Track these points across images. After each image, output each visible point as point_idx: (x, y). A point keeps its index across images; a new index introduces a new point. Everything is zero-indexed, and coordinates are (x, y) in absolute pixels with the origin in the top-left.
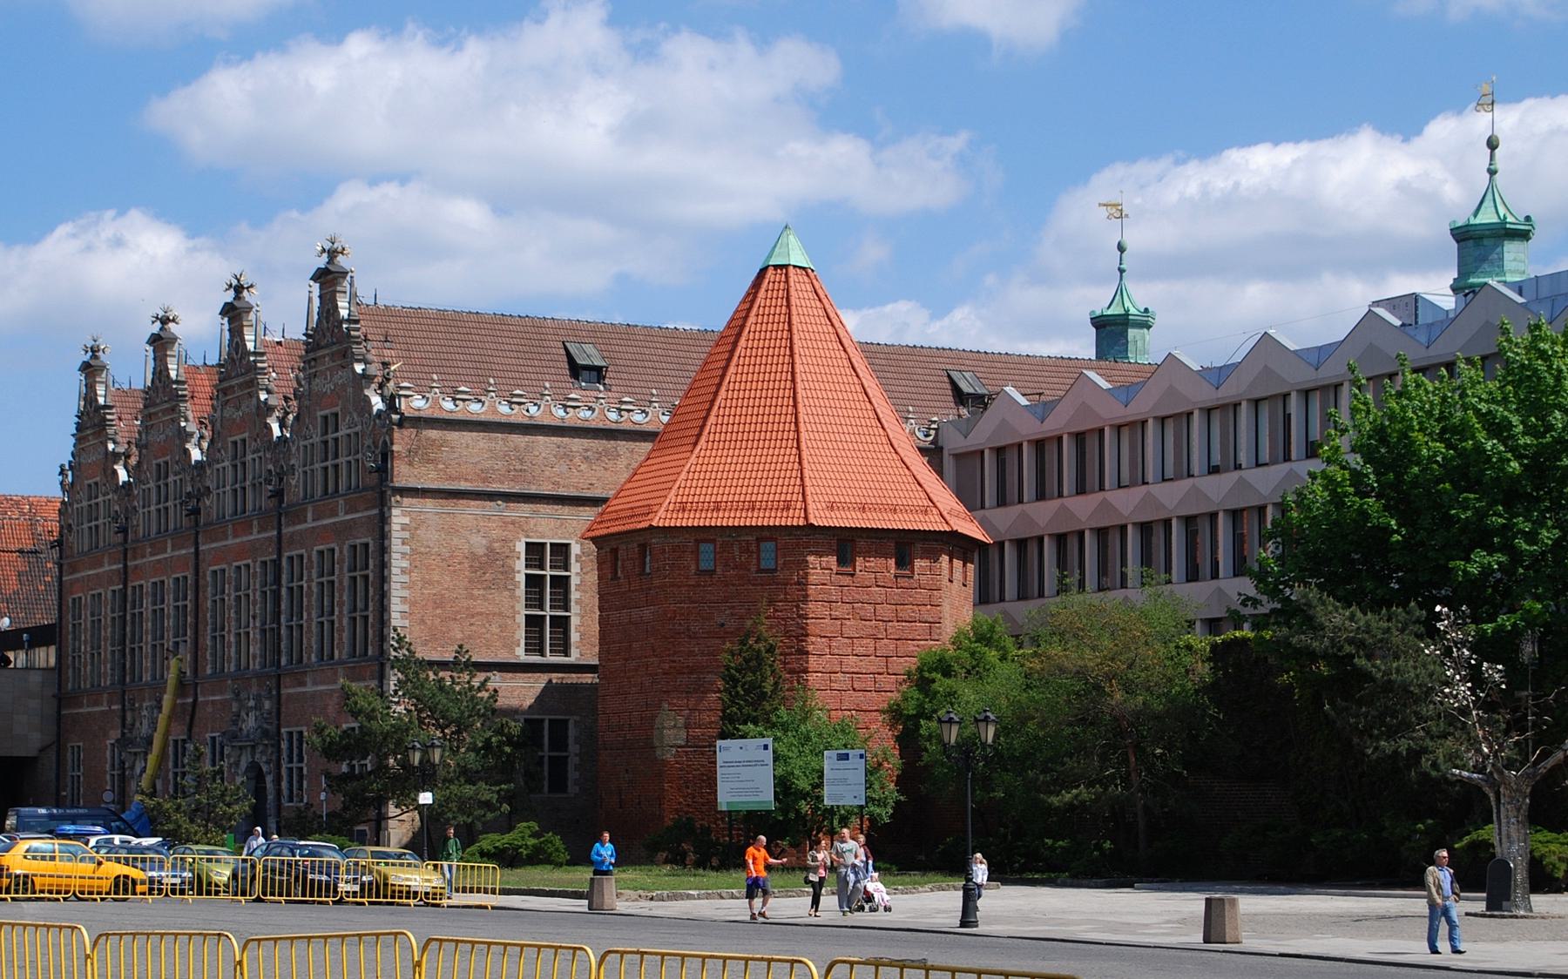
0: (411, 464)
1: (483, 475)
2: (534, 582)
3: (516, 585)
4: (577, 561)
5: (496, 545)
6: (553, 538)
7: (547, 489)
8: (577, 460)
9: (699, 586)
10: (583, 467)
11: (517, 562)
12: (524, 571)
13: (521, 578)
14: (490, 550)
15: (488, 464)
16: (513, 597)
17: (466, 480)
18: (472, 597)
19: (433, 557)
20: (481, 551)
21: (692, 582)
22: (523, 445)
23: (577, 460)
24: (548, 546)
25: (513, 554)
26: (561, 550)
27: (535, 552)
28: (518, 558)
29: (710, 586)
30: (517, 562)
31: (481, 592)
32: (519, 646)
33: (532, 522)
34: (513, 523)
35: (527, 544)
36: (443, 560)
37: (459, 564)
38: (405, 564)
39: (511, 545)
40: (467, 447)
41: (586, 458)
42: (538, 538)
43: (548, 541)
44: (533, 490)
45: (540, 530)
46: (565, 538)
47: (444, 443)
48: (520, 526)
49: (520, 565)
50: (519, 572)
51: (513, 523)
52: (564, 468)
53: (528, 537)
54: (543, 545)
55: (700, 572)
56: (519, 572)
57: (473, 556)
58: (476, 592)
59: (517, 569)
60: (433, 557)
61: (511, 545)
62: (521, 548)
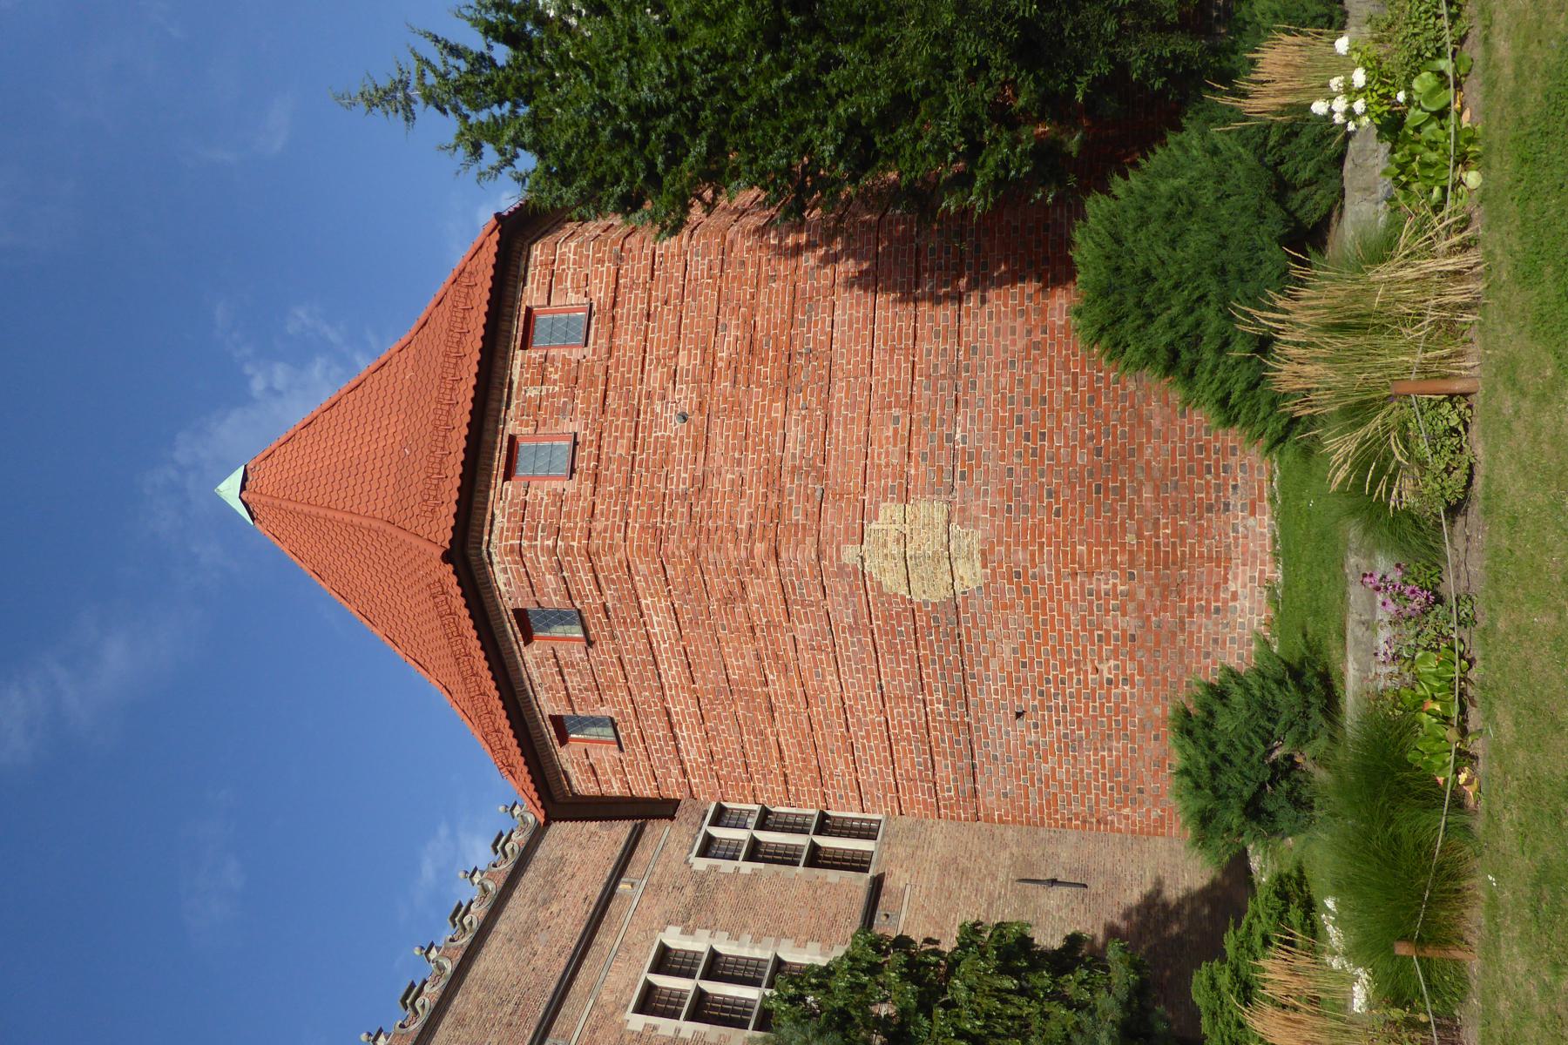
2: (703, 1009)
4: (692, 933)
8: (541, 916)
10: (555, 908)
11: (660, 1032)
23: (541, 916)
24: (661, 981)
26: (665, 961)
27: (649, 1002)
28: (655, 1028)
30: (660, 1032)
41: (545, 902)
42: (632, 991)
45: (621, 987)
48: (605, 1018)
49: (666, 1026)
50: (678, 1030)
53: (626, 1006)
54: (649, 988)
56: (678, 1030)
59: (671, 1033)
61: (627, 1038)
62: (638, 1022)
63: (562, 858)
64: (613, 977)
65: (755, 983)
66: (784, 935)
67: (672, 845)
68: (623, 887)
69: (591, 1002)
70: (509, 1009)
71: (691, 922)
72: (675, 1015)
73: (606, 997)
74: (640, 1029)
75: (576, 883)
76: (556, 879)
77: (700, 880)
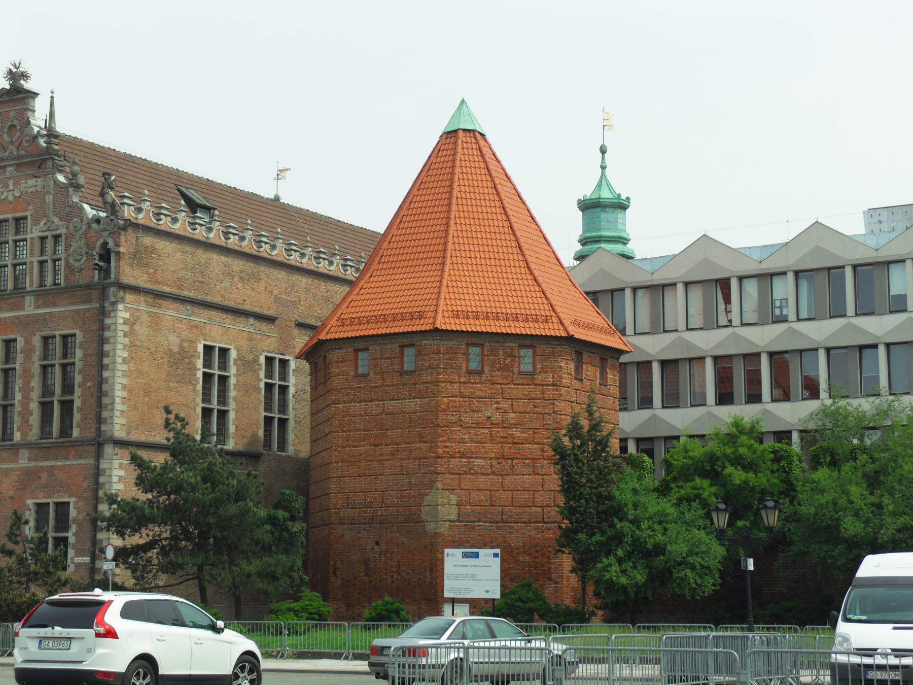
0: (131, 266)
1: (179, 283)
3: (197, 380)
5: (185, 344)
6: (220, 343)
7: (217, 299)
8: (236, 279)
9: (469, 382)
12: (202, 370)
13: (200, 375)
14: (181, 347)
15: (181, 274)
16: (195, 391)
17: (168, 285)
18: (168, 388)
19: (144, 350)
20: (176, 349)
21: (463, 380)
22: (203, 260)
23: (236, 279)
25: (194, 355)
28: (199, 358)
29: (478, 383)
31: (175, 385)
32: (197, 434)
33: (208, 327)
34: (196, 327)
35: (206, 347)
36: (151, 353)
37: (162, 358)
38: (125, 355)
39: (194, 345)
40: (168, 256)
41: (241, 278)
43: (218, 345)
44: (209, 299)
45: (213, 334)
46: (227, 344)
47: (154, 250)
49: (200, 363)
51: (196, 327)
52: (228, 285)
53: (205, 340)
55: (470, 372)
57: (170, 353)
58: (172, 385)
60: (144, 350)
62: (200, 349)
63: (260, 279)
64: (215, 328)
65: (219, 403)
66: (237, 412)
67: (269, 341)
68: (251, 320)
69: (205, 321)
70: (201, 279)
71: (239, 362)
72: (205, 366)
73: (208, 327)
74: (198, 350)
75: (250, 292)
76: (251, 280)
77: (255, 361)
